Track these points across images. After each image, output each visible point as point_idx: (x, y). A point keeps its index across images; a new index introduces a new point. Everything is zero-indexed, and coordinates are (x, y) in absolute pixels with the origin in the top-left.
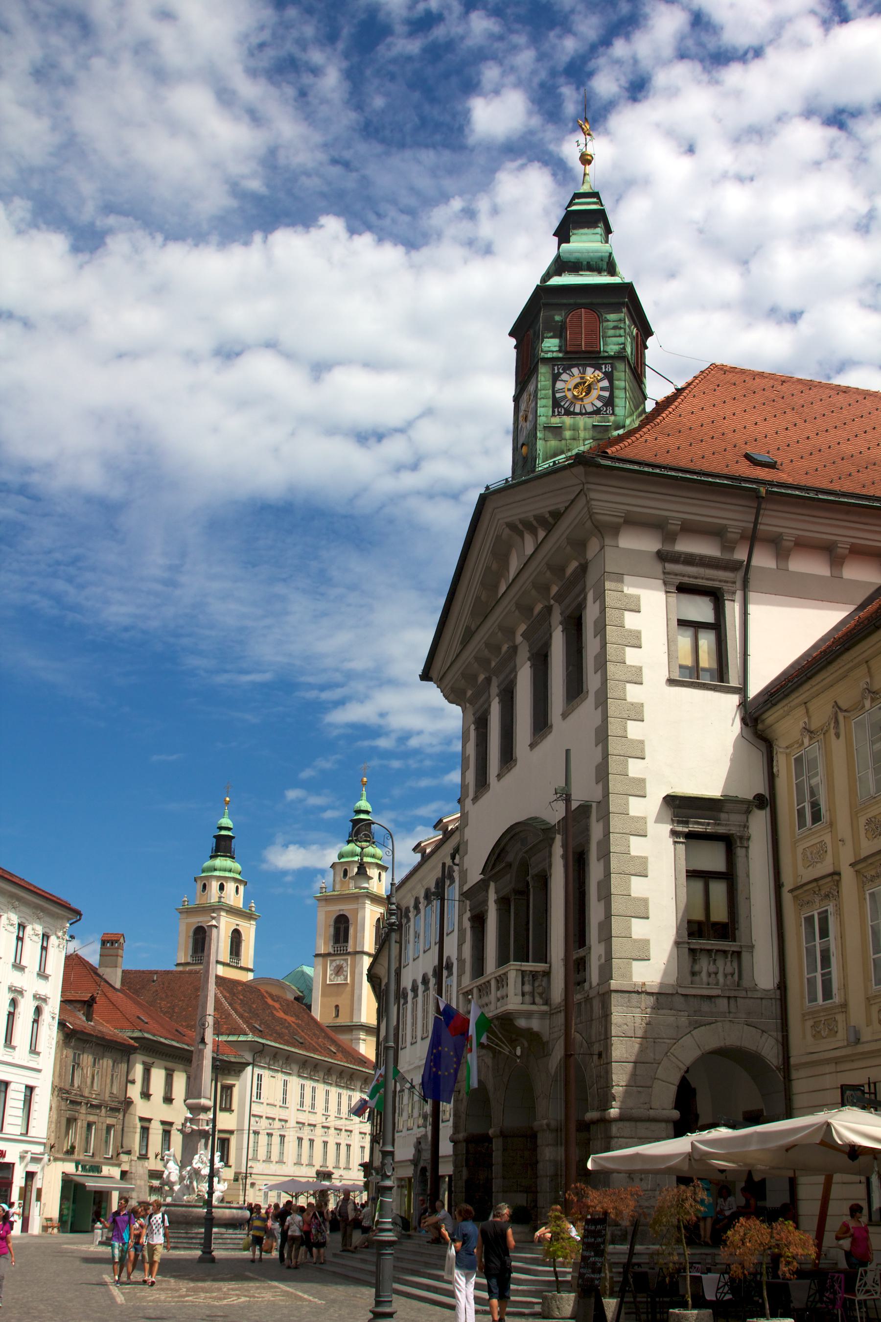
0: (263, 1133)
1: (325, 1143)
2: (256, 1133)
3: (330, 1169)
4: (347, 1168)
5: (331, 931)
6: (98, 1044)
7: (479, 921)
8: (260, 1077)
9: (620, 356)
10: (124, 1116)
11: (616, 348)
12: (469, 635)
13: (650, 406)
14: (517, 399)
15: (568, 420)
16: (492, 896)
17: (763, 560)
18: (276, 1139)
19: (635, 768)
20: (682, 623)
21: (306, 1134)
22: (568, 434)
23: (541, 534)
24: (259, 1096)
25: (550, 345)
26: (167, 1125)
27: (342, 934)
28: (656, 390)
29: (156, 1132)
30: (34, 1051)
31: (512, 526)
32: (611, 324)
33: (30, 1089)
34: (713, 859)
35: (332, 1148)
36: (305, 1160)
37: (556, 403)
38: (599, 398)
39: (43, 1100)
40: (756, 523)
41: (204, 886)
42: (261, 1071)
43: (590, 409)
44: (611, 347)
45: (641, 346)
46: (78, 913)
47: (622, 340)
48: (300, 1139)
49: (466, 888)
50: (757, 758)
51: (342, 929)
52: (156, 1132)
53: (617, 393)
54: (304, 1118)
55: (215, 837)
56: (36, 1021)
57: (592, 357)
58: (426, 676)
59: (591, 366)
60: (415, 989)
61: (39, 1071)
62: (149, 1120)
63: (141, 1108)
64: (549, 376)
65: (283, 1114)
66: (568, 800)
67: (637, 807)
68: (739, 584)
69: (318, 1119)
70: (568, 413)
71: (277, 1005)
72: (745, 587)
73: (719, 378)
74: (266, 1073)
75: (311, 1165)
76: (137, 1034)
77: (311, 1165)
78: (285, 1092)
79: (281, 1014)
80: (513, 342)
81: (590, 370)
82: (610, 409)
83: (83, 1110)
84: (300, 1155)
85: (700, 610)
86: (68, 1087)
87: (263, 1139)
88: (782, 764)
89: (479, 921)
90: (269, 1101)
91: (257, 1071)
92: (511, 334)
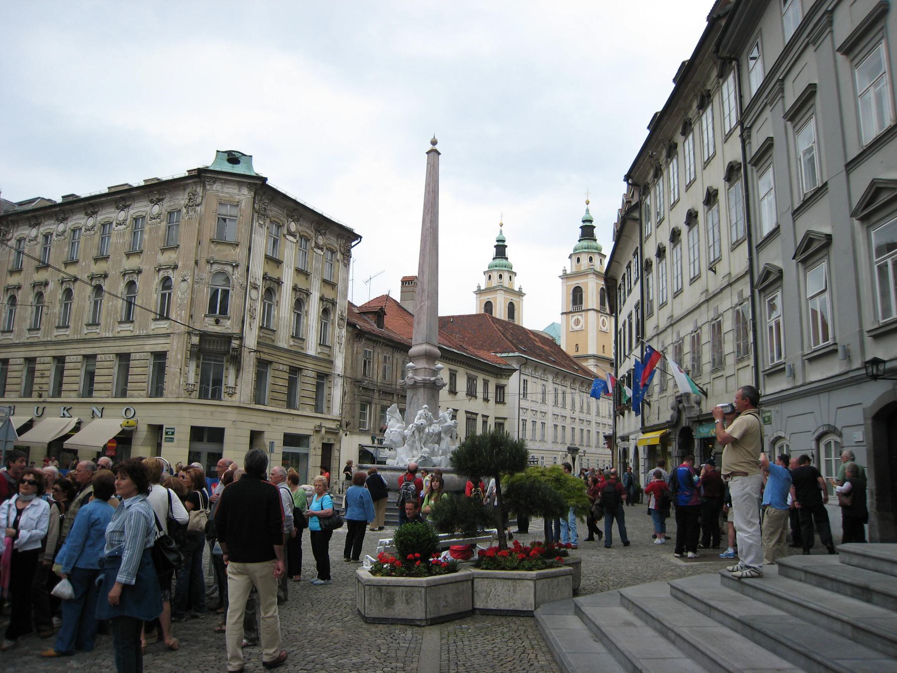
1: (573, 429)
2: (524, 421)
3: (577, 446)
4: (588, 446)
5: (571, 297)
6: (387, 345)
8: (525, 381)
18: (539, 425)
21: (560, 423)
24: (525, 395)
35: (577, 432)
36: (559, 440)
41: (490, 277)
42: (526, 377)
48: (556, 426)
54: (557, 411)
65: (544, 408)
69: (567, 412)
71: (537, 339)
74: (529, 379)
75: (564, 443)
77: (564, 443)
79: (540, 345)
83: (376, 395)
84: (556, 437)
86: (360, 376)
90: (534, 399)
91: (523, 377)
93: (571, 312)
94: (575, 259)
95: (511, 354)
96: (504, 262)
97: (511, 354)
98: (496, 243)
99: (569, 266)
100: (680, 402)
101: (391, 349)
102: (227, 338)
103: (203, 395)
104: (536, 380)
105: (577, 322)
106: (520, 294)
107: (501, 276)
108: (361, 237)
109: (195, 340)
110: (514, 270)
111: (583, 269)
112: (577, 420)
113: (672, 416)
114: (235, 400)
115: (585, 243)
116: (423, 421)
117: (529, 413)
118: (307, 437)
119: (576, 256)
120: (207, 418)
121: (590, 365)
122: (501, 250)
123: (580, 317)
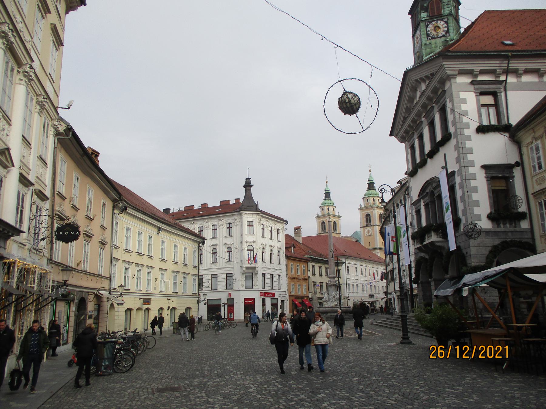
2: (349, 284)
5: (365, 219)
7: (418, 212)
8: (348, 267)
9: (450, 14)
11: (448, 12)
12: (405, 119)
13: (462, 30)
14: (413, 37)
15: (433, 41)
16: (422, 204)
17: (511, 79)
18: (355, 286)
19: (470, 157)
20: (483, 106)
22: (433, 46)
23: (427, 82)
24: (348, 273)
25: (424, 15)
28: (464, 24)
30: (279, 263)
31: (416, 81)
32: (446, 4)
34: (501, 186)
37: (428, 36)
38: (444, 31)
39: (284, 279)
40: (508, 66)
43: (440, 35)
44: (446, 12)
45: (457, 9)
46: (287, 222)
47: (450, 8)
49: (412, 202)
50: (513, 149)
53: (450, 28)
56: (279, 255)
57: (440, 17)
58: (391, 135)
59: (439, 20)
63: (313, 279)
64: (425, 26)
66: (447, 170)
67: (471, 170)
68: (502, 90)
70: (433, 38)
72: (505, 90)
73: (488, 15)
76: (309, 257)
78: (356, 271)
80: (410, 16)
81: (439, 22)
82: (448, 35)
85: (489, 100)
87: (351, 286)
88: (524, 150)
89: (418, 212)
92: (409, 14)
93: (365, 227)
94: (366, 200)
96: (329, 201)
102: (254, 268)
105: (369, 232)
106: (338, 217)
109: (244, 269)
114: (257, 287)
119: (366, 198)
120: (249, 294)
122: (327, 196)
123: (370, 229)
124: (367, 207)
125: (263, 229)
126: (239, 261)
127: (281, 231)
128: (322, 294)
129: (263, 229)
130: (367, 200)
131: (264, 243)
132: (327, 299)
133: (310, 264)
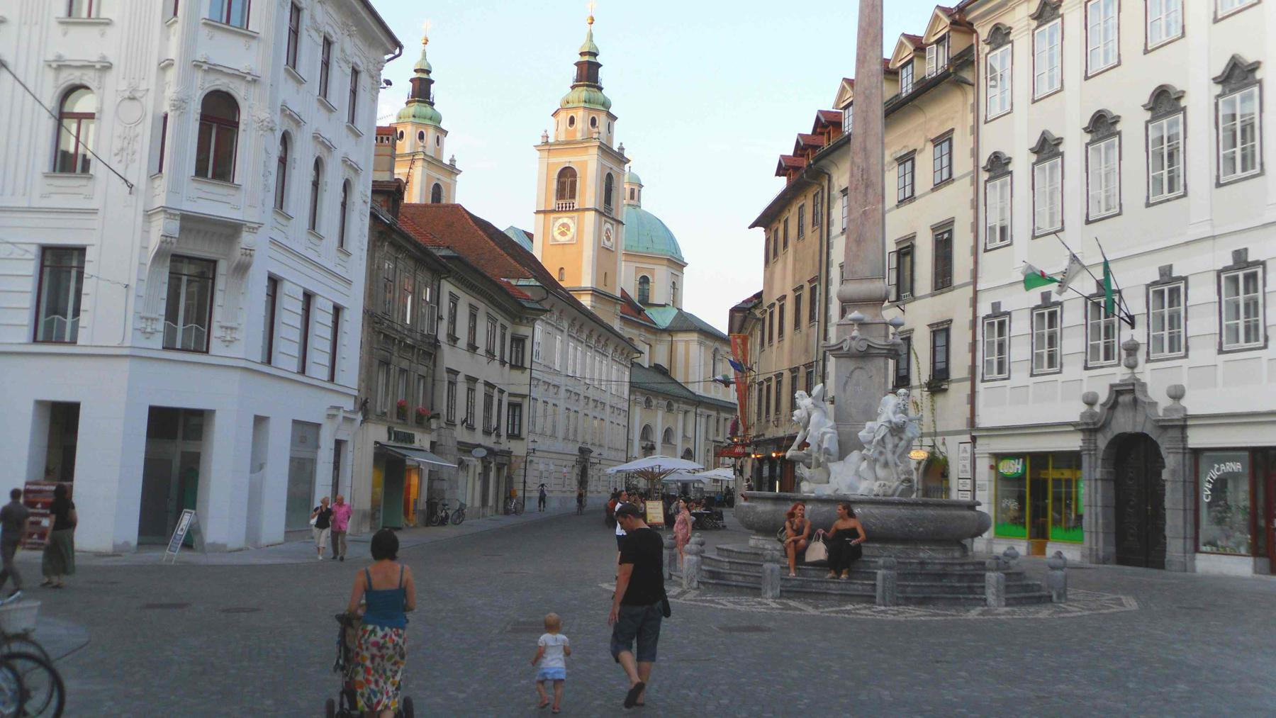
0: (540, 401)
6: (412, 257)
10: (435, 365)
26: (471, 380)
27: (568, 189)
29: (462, 388)
33: (337, 310)
46: (397, 44)
51: (568, 183)
52: (462, 388)
55: (412, 80)
60: (1047, 148)
61: (349, 282)
62: (456, 373)
63: (452, 357)
75: (575, 441)
77: (575, 441)
94: (564, 117)
95: (522, 282)
96: (427, 110)
97: (522, 282)
98: (415, 75)
99: (555, 130)
100: (1119, 393)
101: (411, 263)
102: (230, 230)
103: (169, 346)
104: (550, 329)
106: (452, 170)
107: (421, 136)
108: (401, 47)
109: (175, 226)
110: (443, 125)
111: (579, 137)
112: (591, 403)
113: (1083, 415)
114: (237, 351)
115: (583, 93)
116: (899, 418)
117: (542, 388)
118: (318, 426)
120: (182, 386)
121: (586, 301)
124: (568, 143)
125: (294, 33)
126: (138, 172)
127: (364, 79)
128: (471, 428)
129: (294, 33)
130: (572, 121)
131: (296, 107)
132: (830, 442)
133: (447, 287)
